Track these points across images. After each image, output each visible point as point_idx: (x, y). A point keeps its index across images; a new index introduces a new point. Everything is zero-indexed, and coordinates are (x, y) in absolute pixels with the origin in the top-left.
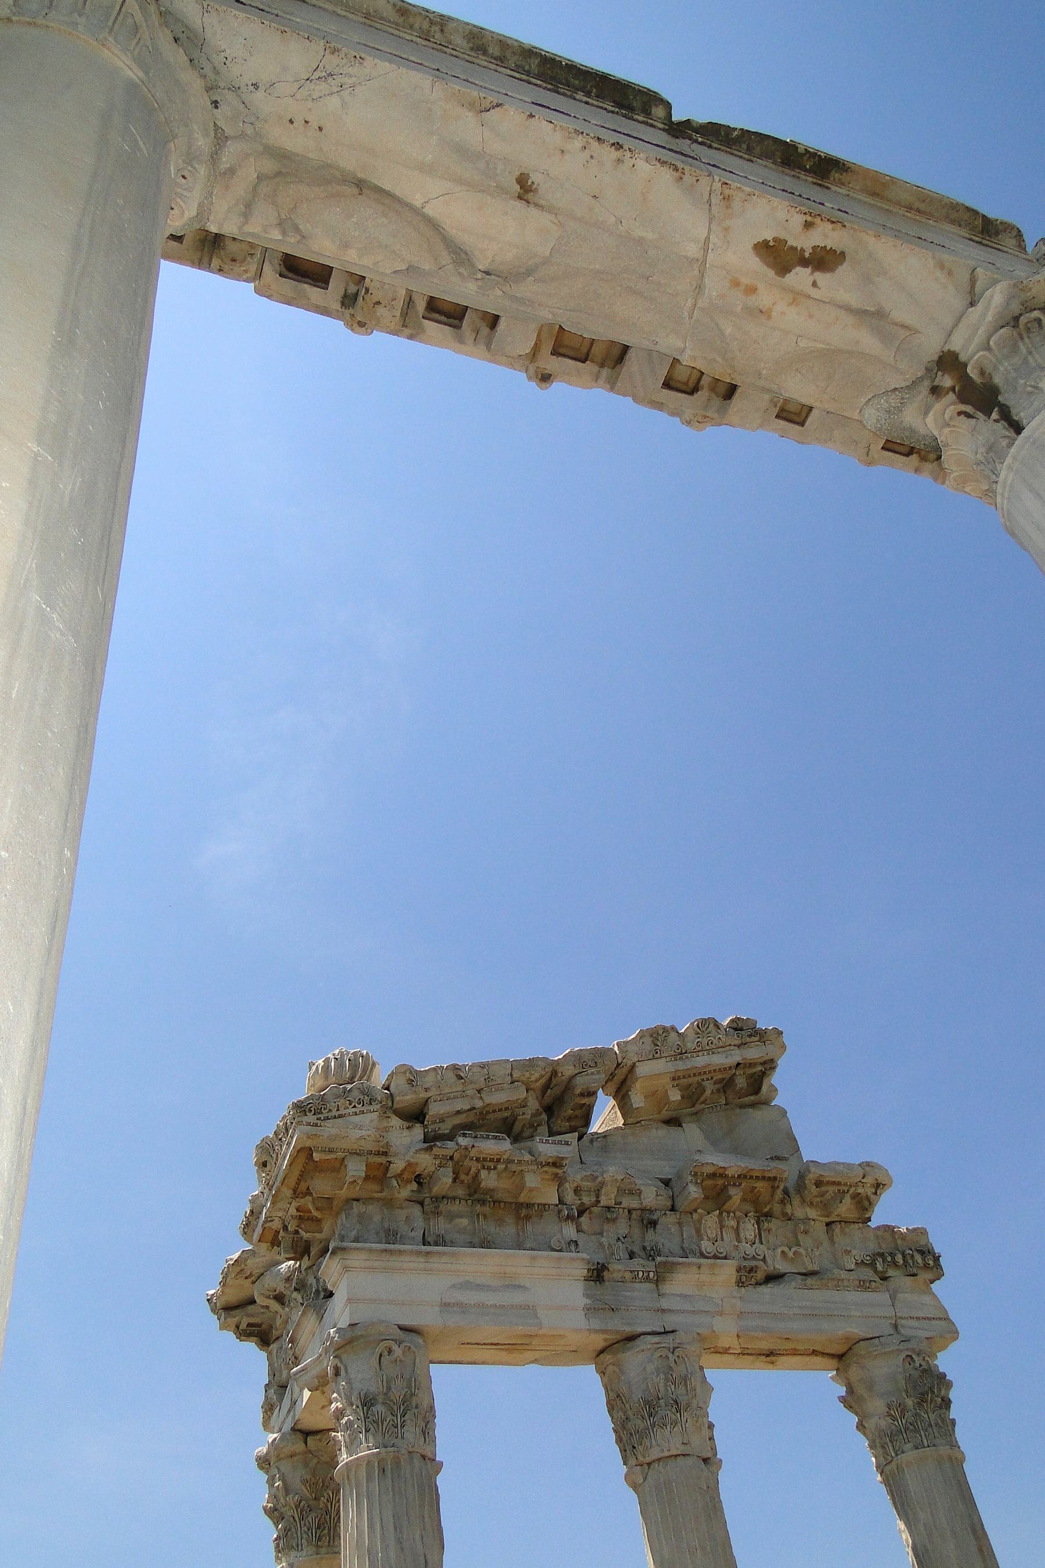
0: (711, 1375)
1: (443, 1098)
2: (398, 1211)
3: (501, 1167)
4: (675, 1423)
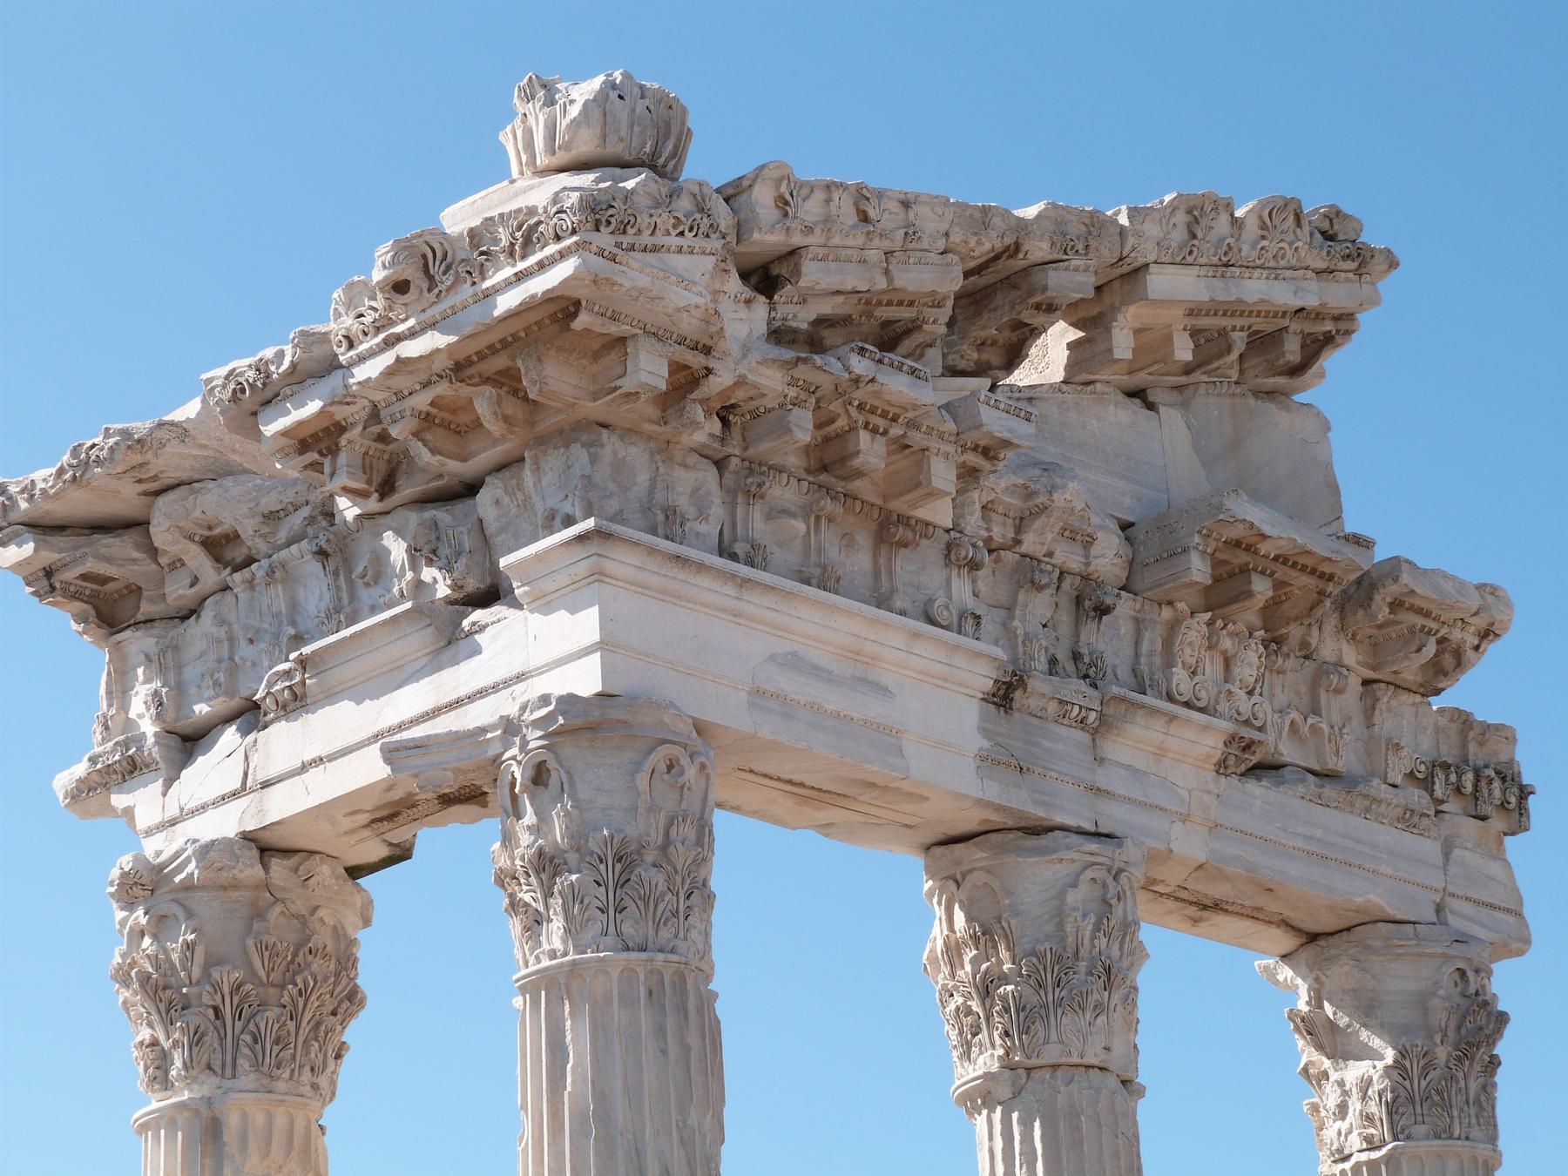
0: (1150, 934)
1: (831, 255)
2: (679, 472)
3: (896, 431)
4: (1099, 1009)
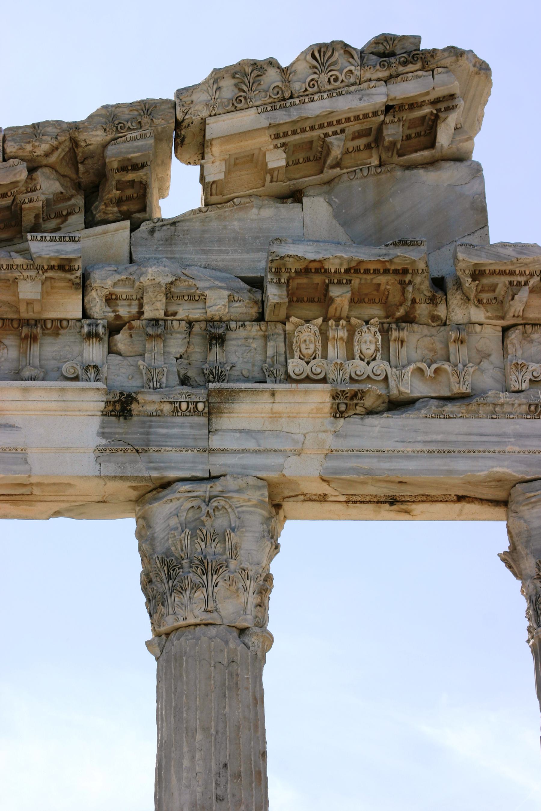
4: (195, 587)
